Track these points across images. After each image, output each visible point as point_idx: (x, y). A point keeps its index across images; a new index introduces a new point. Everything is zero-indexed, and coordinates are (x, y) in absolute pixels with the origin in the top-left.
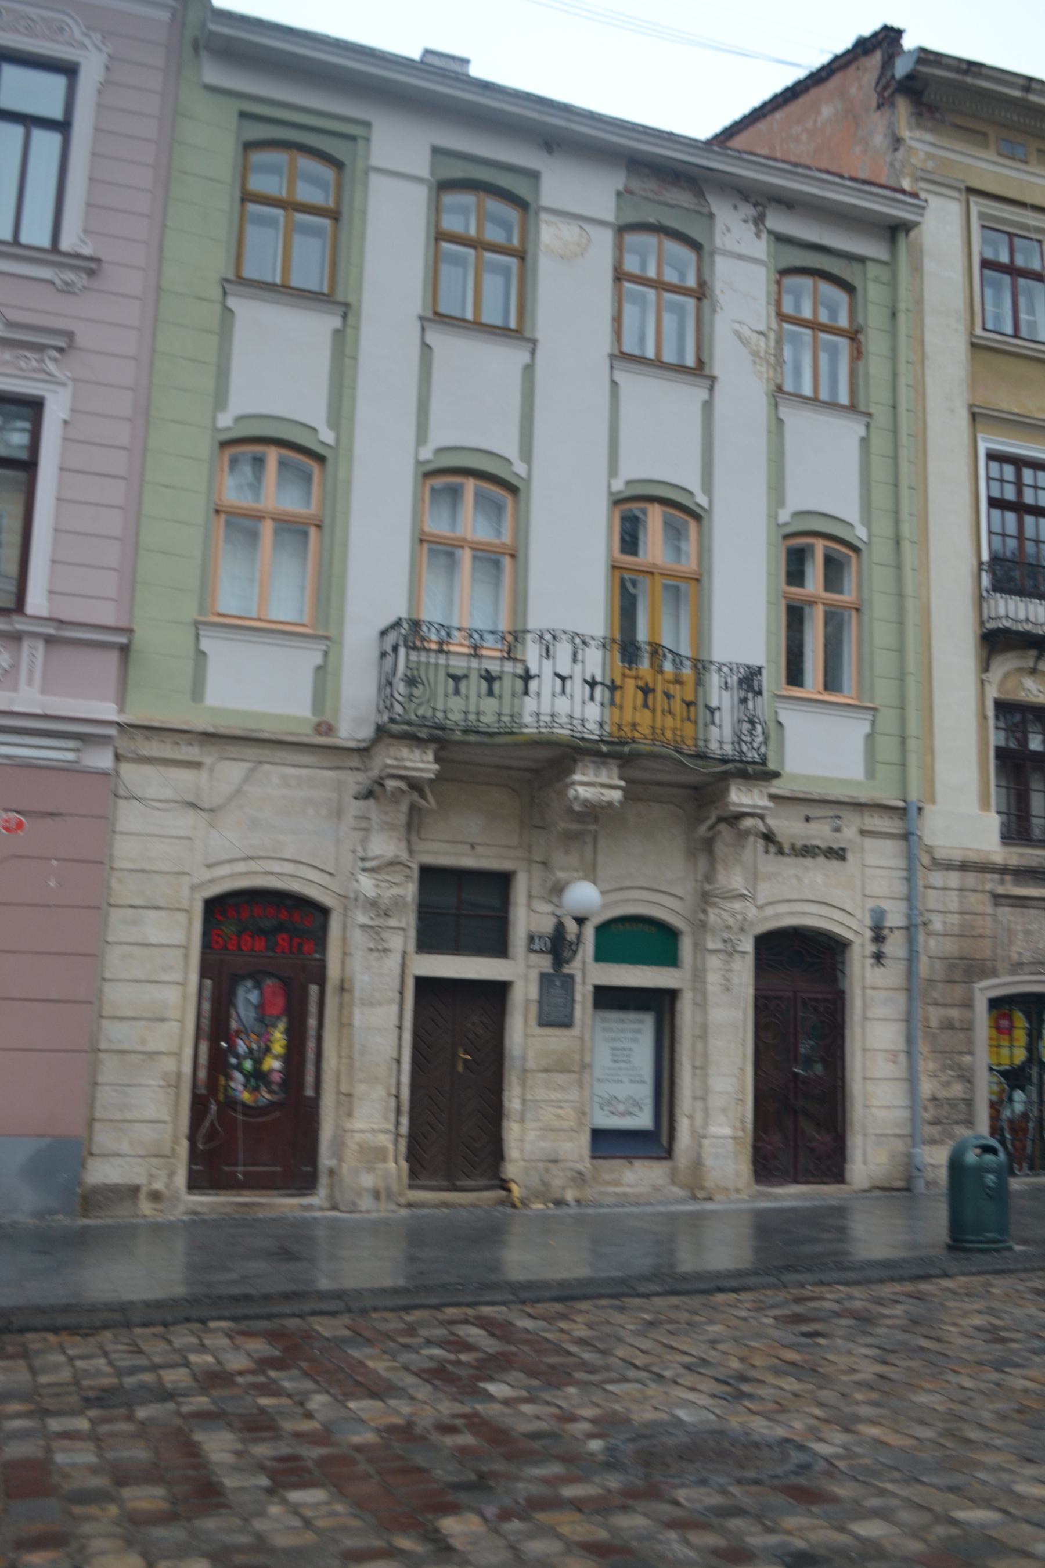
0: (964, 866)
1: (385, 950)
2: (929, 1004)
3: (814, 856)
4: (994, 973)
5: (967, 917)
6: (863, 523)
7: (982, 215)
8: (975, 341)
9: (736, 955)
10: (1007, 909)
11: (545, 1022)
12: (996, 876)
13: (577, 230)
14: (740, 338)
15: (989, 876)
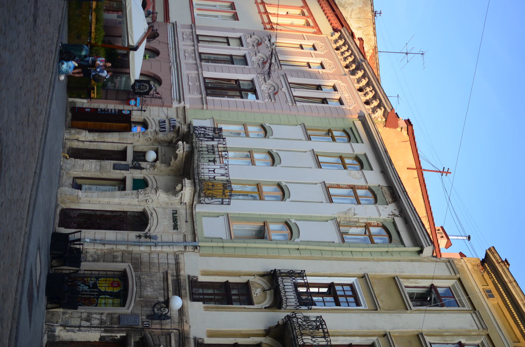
0: (177, 264)
1: (134, 135)
2: (122, 253)
3: (174, 222)
4: (135, 271)
5: (157, 265)
6: (301, 241)
7: (453, 285)
8: (396, 277)
9: (137, 196)
10: (162, 276)
11: (114, 165)
12: (175, 274)
13: (360, 177)
14: (349, 209)
15: (175, 272)
